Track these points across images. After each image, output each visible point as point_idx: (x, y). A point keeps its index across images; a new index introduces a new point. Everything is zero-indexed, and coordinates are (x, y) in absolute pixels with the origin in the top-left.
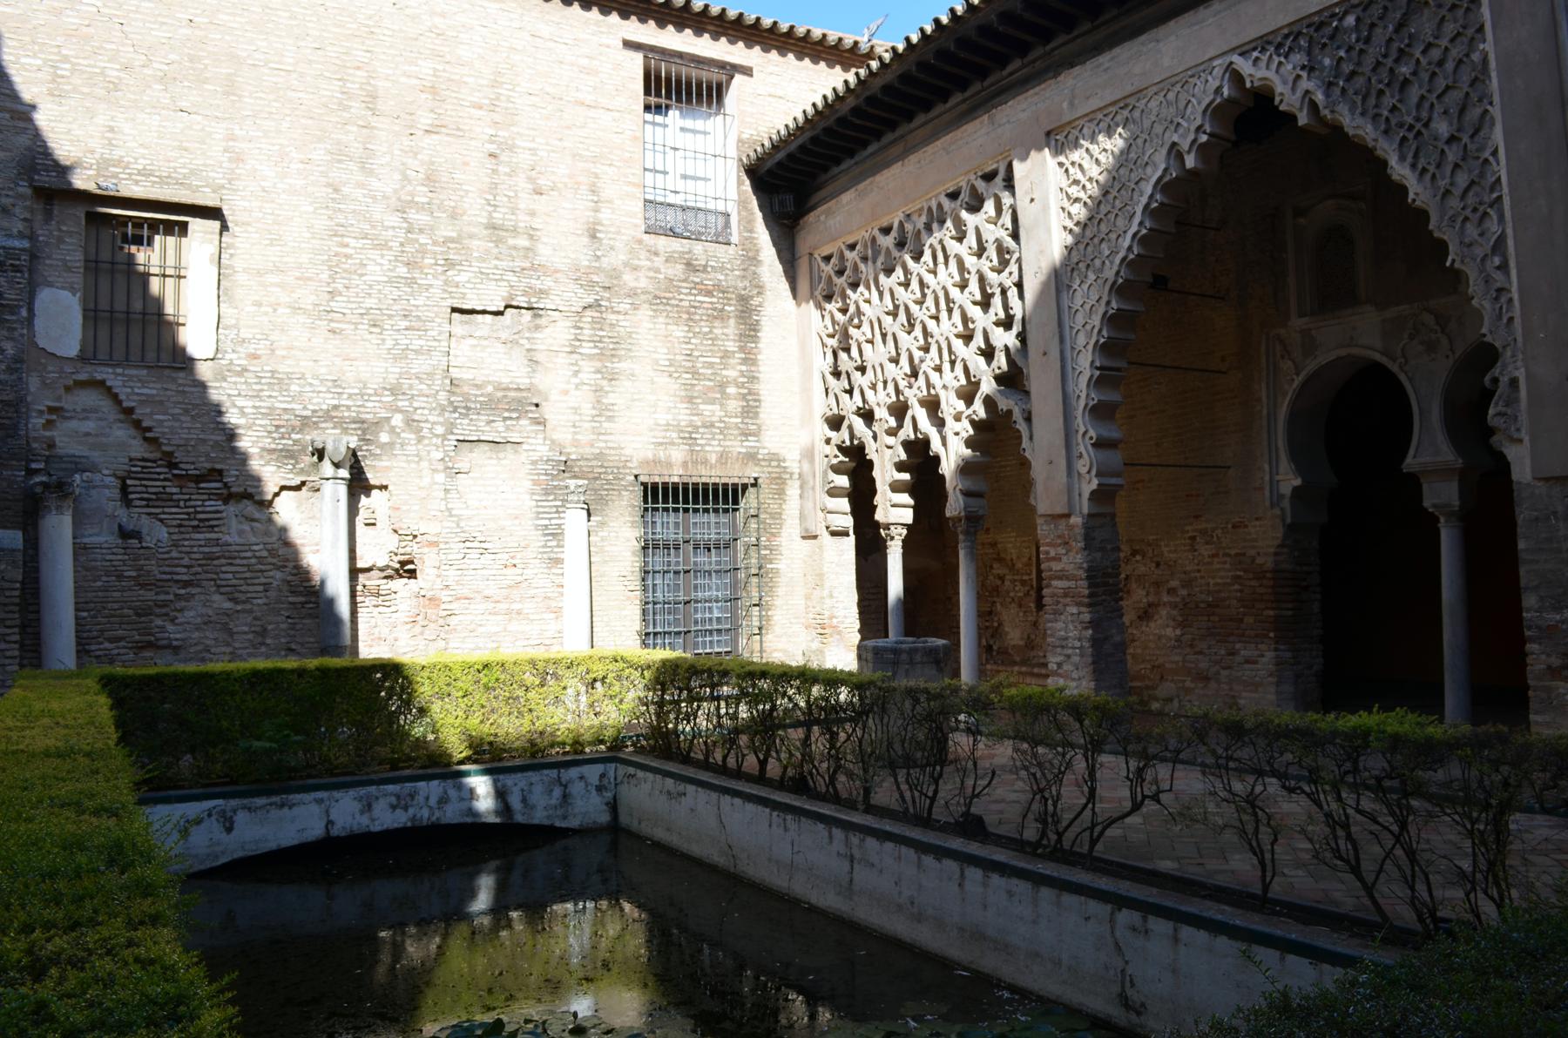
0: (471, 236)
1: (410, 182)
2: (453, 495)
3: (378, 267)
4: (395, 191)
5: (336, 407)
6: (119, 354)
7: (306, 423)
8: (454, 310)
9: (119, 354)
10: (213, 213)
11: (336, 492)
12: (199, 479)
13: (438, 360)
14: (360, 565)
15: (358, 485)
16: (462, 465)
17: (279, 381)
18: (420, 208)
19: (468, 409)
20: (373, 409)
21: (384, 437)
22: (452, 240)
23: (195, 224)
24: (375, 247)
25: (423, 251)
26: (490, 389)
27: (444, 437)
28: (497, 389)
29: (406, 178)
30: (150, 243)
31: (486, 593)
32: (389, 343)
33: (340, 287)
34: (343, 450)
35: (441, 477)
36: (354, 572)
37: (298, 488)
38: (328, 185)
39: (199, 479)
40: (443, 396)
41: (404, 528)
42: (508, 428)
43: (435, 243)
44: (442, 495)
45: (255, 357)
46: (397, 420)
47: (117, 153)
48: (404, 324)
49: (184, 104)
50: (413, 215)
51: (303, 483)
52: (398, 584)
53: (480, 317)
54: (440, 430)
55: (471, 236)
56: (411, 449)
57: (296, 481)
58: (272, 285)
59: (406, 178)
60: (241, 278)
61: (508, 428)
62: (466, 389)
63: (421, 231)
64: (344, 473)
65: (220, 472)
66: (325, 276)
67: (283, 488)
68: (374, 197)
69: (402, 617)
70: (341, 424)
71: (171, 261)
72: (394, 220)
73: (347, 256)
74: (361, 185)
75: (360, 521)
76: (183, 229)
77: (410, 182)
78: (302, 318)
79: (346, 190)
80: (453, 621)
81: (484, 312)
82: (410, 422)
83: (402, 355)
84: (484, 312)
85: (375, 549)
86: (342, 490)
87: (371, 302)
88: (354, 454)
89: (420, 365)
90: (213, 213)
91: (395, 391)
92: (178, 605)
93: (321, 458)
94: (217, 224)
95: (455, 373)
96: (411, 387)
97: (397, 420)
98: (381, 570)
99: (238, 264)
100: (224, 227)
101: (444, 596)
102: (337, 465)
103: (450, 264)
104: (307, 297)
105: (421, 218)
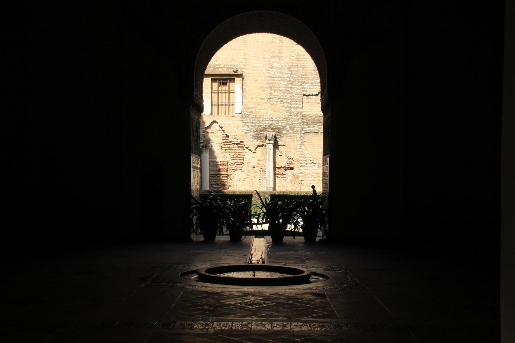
0: (309, 74)
1: (292, 60)
2: (303, 147)
3: (283, 85)
4: (288, 63)
5: (271, 124)
6: (220, 114)
7: (264, 129)
8: (304, 95)
9: (220, 114)
10: (240, 76)
11: (270, 147)
12: (238, 144)
13: (299, 110)
14: (277, 166)
15: (276, 146)
16: (306, 139)
17: (257, 118)
18: (295, 67)
19: (307, 123)
20: (281, 124)
21: (284, 132)
22: (304, 75)
23: (237, 79)
24: (282, 80)
25: (295, 80)
26: (314, 117)
27: (301, 131)
28: (316, 117)
29: (291, 59)
30: (226, 84)
31: (313, 175)
32: (286, 106)
33: (273, 92)
34: (271, 136)
35: (299, 143)
36: (275, 168)
37: (262, 146)
38: (270, 64)
39: (238, 144)
40: (300, 120)
41: (289, 156)
42: (319, 128)
43: (298, 77)
44: (300, 147)
45: (250, 112)
46: (288, 127)
47: (218, 62)
48: (290, 100)
49: (233, 47)
50: (293, 70)
51: (263, 145)
52: (288, 172)
53: (311, 97)
54: (299, 129)
55: (309, 74)
56: (291, 135)
57: (262, 144)
58: (255, 93)
59: (291, 59)
60: (248, 92)
61: (319, 128)
62: (307, 117)
63: (295, 74)
64: (272, 142)
65: (243, 142)
66: (269, 89)
67: (258, 146)
68: (282, 66)
69: (289, 180)
70: (273, 129)
71: (231, 89)
72: (287, 71)
73: (275, 83)
74: (278, 63)
75: (277, 155)
76: (234, 80)
77: (292, 60)
78: (263, 101)
79: (274, 65)
80: (303, 182)
81: (312, 95)
82: (291, 128)
83: (289, 109)
84: (312, 95)
85: (281, 162)
86: (271, 147)
87: (281, 95)
88: (275, 137)
89: (294, 111)
90: (240, 76)
91: (287, 119)
92: (232, 176)
93: (266, 139)
94: (241, 79)
95: (304, 113)
96: (292, 118)
97: (288, 127)
98: (284, 168)
99: (247, 88)
100: (243, 80)
101: (300, 175)
102: (270, 140)
103: (303, 82)
104: (264, 95)
105: (295, 70)
